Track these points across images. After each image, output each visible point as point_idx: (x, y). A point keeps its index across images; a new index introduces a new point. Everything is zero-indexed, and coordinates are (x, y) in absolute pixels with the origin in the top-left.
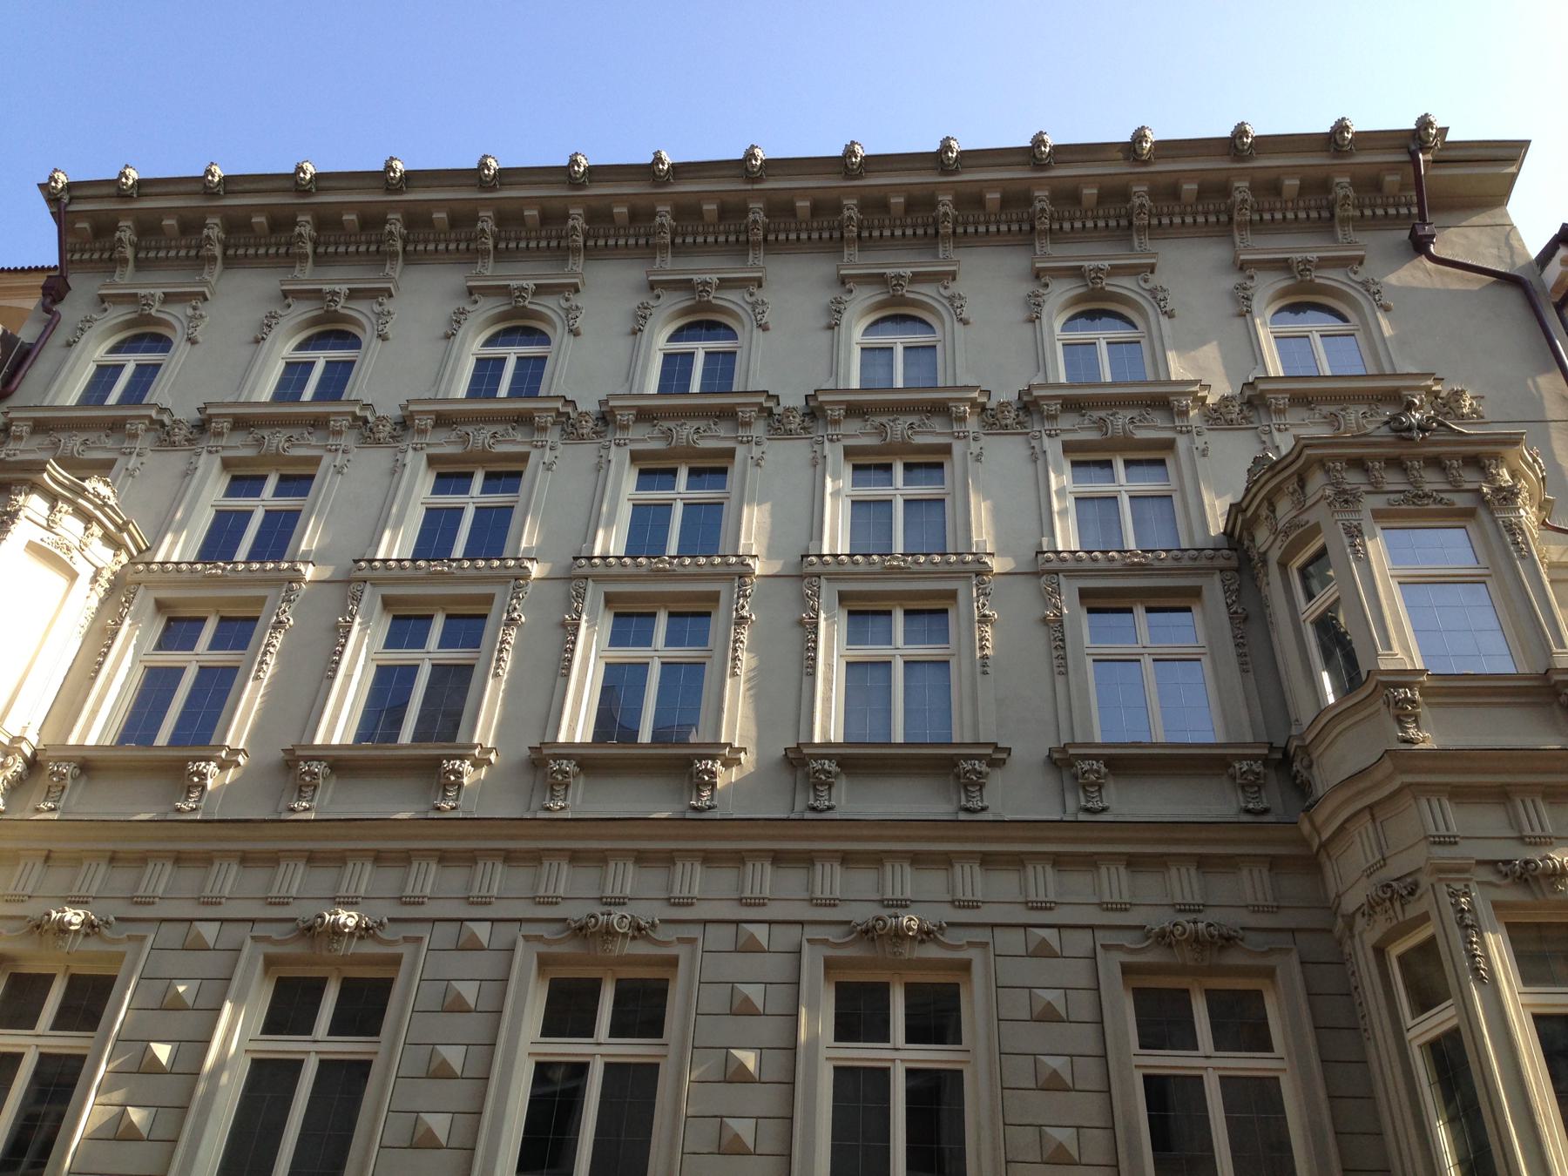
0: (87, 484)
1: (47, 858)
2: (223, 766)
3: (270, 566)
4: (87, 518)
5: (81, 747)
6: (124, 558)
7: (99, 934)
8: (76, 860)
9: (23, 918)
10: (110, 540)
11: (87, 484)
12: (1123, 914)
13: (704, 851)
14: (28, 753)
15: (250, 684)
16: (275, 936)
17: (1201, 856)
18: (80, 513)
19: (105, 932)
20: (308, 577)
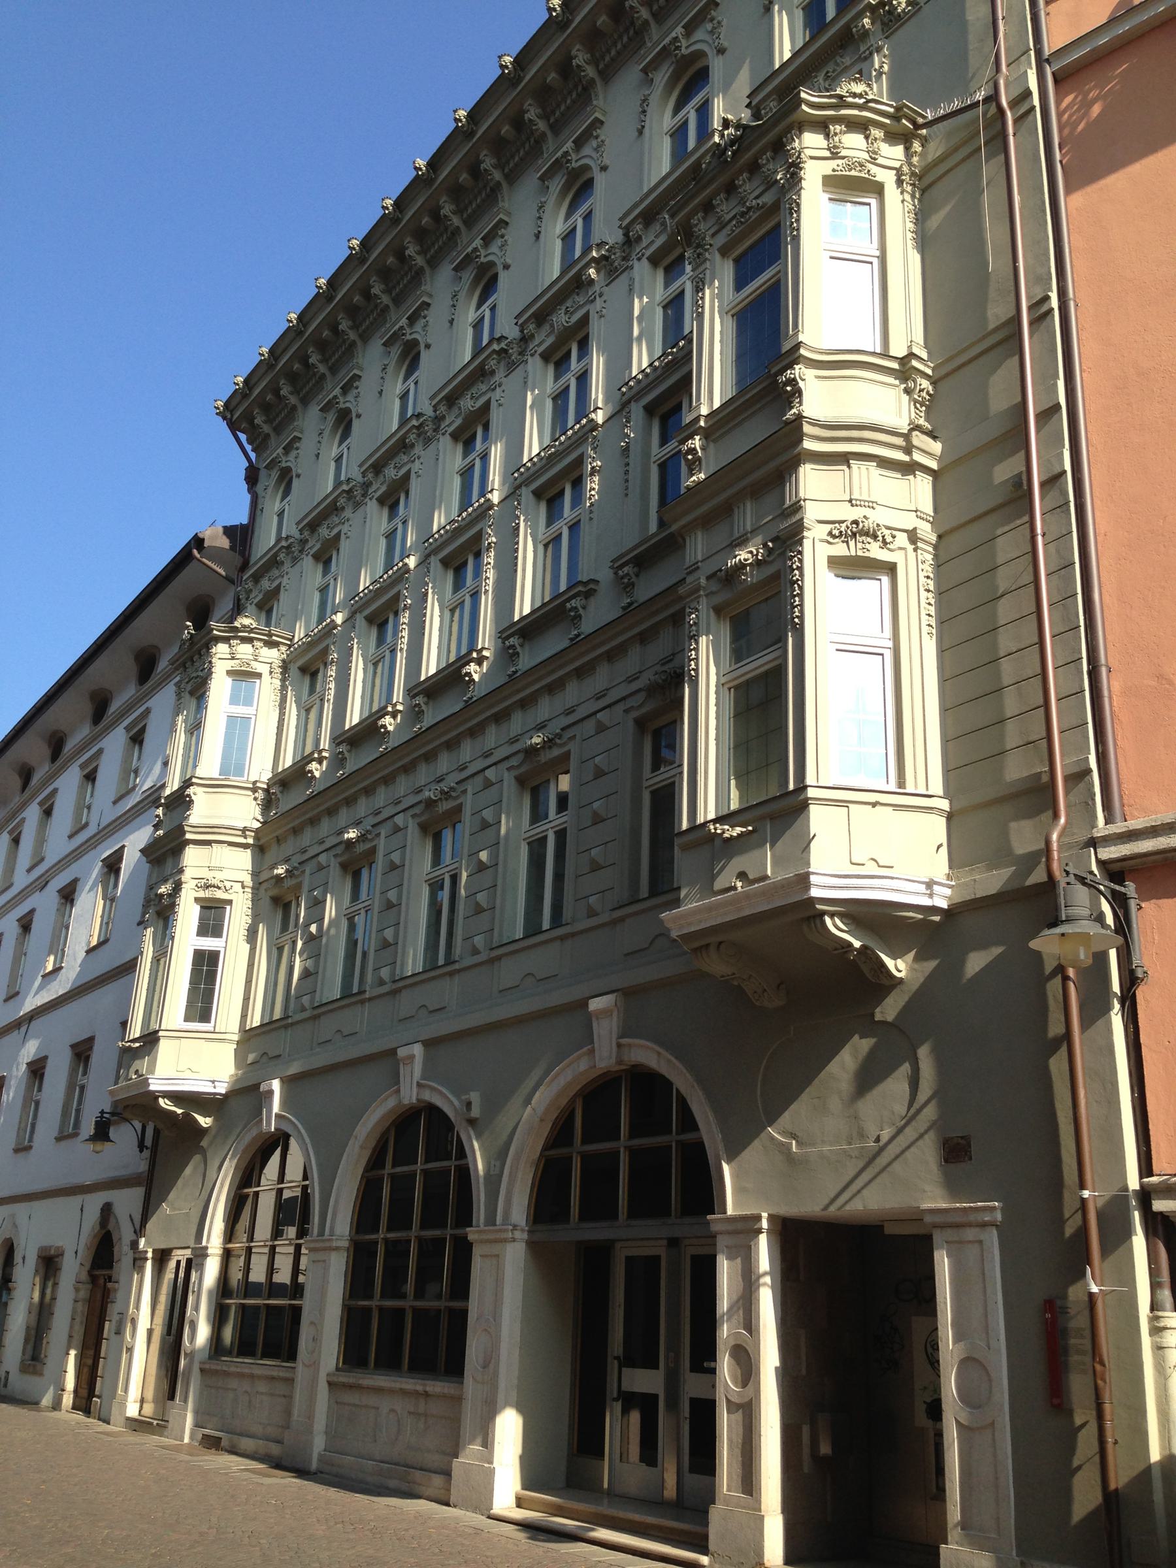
0: (237, 624)
1: (278, 841)
2: (480, 664)
3: (470, 509)
4: (250, 640)
5: (522, 618)
6: (283, 648)
7: (556, 744)
8: (296, 831)
9: (420, 802)
10: (271, 644)
11: (237, 624)
12: (637, 682)
13: (546, 685)
14: (265, 786)
15: (483, 597)
16: (635, 705)
17: (576, 669)
18: (245, 640)
19: (453, 794)
20: (600, 421)
